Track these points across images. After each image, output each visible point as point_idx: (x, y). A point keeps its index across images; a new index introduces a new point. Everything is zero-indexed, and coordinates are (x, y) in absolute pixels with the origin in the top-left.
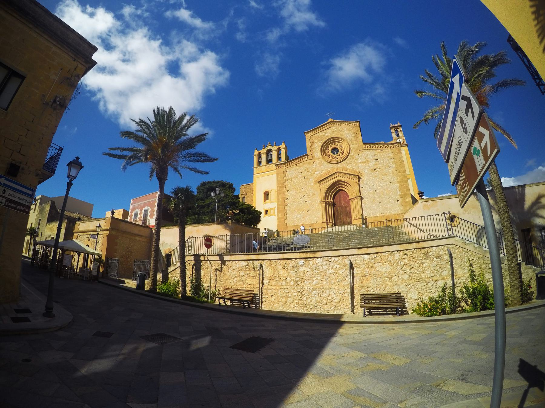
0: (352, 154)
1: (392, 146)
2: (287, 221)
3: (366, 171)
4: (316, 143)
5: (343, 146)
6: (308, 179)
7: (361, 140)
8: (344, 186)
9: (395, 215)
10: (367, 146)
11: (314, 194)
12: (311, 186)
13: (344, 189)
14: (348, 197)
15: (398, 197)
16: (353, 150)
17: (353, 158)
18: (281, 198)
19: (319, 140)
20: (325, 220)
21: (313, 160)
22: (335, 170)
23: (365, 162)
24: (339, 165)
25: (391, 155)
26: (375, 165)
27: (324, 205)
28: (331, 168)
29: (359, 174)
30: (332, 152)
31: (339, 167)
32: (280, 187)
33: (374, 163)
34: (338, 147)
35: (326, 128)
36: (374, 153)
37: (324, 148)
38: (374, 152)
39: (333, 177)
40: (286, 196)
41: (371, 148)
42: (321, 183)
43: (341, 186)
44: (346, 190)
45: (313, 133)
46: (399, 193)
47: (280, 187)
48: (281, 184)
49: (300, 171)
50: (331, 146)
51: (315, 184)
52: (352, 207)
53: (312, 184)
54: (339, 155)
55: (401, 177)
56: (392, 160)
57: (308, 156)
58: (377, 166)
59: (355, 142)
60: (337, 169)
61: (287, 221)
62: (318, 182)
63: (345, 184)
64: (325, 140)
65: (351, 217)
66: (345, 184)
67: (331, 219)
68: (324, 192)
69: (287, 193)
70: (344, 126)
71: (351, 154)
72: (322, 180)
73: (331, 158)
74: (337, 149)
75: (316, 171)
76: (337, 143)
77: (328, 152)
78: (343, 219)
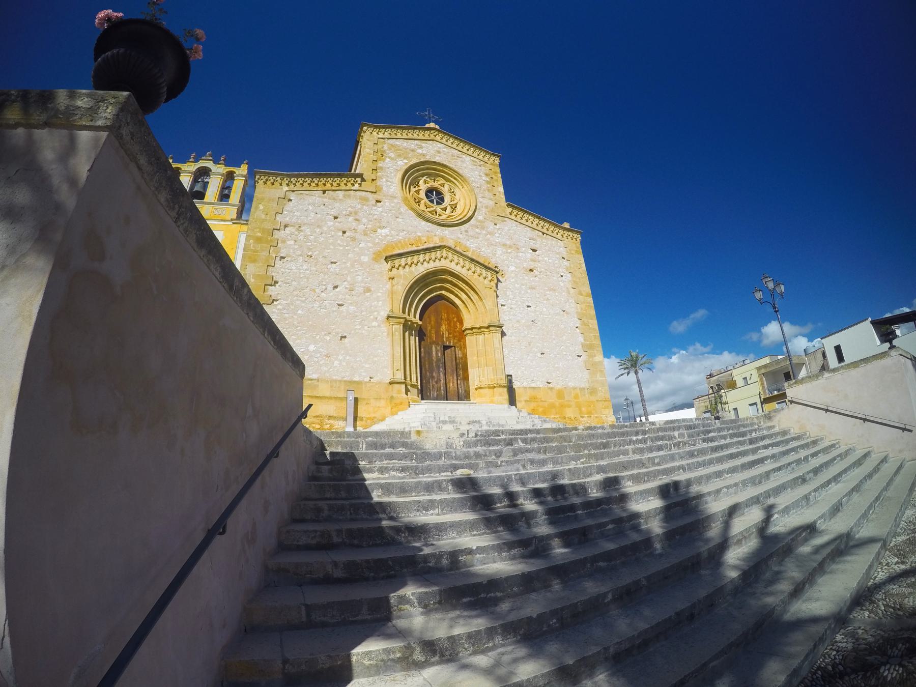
0: (480, 218)
1: (566, 233)
3: (512, 268)
4: (392, 159)
7: (503, 196)
8: (456, 290)
9: (575, 388)
10: (515, 212)
14: (461, 323)
15: (579, 350)
16: (484, 210)
17: (483, 228)
19: (400, 156)
20: (400, 376)
21: (376, 197)
24: (447, 231)
26: (534, 261)
30: (426, 195)
31: (449, 236)
32: (258, 240)
33: (529, 256)
34: (445, 190)
35: (421, 137)
37: (411, 175)
38: (529, 233)
39: (433, 255)
40: (274, 273)
41: (523, 221)
42: (397, 262)
43: (448, 286)
45: (387, 135)
47: (258, 240)
48: (263, 231)
49: (334, 212)
50: (425, 182)
52: (469, 351)
53: (365, 259)
54: (445, 209)
55: (583, 306)
57: (363, 180)
59: (487, 194)
60: (442, 239)
63: (460, 284)
64: (414, 161)
65: (466, 378)
66: (460, 284)
67: (415, 378)
68: (401, 288)
69: (279, 263)
70: (465, 150)
71: (479, 216)
72: (400, 255)
74: (439, 193)
76: (442, 181)
77: (418, 192)
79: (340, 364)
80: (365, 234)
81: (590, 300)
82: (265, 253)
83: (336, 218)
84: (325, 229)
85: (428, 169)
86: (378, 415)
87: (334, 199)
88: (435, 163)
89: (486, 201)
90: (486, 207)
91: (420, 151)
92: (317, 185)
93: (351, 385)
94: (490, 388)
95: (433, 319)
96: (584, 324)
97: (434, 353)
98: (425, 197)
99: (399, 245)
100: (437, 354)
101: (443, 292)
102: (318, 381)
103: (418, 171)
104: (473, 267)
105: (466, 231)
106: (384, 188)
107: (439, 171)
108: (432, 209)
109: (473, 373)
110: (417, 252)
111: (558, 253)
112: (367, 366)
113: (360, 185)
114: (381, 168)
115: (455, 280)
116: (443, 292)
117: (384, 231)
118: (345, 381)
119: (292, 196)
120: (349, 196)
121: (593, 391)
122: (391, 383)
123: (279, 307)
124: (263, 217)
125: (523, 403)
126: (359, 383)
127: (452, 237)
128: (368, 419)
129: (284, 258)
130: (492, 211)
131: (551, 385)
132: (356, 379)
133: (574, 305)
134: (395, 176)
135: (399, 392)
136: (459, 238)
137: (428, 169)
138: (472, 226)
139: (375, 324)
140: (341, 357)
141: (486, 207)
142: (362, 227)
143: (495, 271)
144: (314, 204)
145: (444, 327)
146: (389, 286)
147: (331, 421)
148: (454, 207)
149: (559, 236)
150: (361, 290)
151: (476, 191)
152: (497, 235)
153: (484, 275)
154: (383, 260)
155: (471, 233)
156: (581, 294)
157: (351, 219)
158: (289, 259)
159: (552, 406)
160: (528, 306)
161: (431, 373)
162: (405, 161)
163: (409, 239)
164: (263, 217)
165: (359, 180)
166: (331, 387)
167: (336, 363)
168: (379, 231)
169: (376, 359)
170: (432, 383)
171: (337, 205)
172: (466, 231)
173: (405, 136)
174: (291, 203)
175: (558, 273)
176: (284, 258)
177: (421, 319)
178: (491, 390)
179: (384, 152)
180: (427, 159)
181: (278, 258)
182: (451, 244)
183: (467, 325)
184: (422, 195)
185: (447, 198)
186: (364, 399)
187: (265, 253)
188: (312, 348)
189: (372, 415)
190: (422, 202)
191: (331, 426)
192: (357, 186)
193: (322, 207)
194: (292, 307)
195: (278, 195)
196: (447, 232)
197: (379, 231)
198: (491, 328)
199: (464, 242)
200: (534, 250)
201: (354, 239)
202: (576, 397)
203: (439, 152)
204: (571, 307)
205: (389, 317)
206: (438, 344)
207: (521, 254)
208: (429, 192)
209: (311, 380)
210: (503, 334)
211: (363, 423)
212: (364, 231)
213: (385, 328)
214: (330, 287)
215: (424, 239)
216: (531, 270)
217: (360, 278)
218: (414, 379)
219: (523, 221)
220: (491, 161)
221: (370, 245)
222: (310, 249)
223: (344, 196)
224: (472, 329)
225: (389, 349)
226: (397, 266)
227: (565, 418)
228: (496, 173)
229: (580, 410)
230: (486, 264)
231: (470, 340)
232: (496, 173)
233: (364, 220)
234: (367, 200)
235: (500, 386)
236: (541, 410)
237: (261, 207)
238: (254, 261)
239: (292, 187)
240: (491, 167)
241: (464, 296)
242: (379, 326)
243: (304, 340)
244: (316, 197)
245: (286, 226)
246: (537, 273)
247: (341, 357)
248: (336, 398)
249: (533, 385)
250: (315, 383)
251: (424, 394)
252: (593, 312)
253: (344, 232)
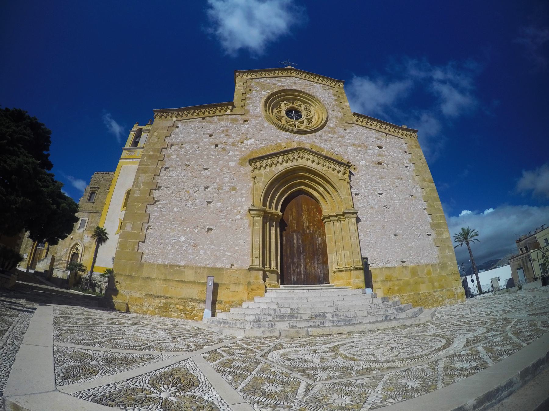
0: (332, 125)
1: (405, 133)
2: (144, 248)
3: (363, 163)
6: (224, 150)
8: (314, 184)
9: (427, 265)
11: (234, 189)
12: (229, 168)
13: (311, 191)
14: (320, 212)
15: (428, 229)
16: (334, 120)
17: (335, 133)
18: (145, 184)
19: (264, 88)
20: (258, 263)
21: (243, 117)
22: (295, 145)
24: (303, 138)
26: (380, 155)
27: (258, 220)
28: (284, 139)
30: (287, 114)
31: (306, 141)
33: (376, 152)
35: (280, 75)
36: (374, 136)
37: (272, 101)
40: (158, 180)
41: (368, 125)
42: (259, 164)
43: (306, 181)
45: (254, 76)
46: (429, 219)
47: (150, 157)
50: (285, 105)
51: (241, 164)
52: (329, 237)
55: (428, 190)
57: (234, 107)
59: (336, 108)
60: (300, 143)
61: (144, 248)
62: (252, 161)
65: (325, 262)
67: (275, 264)
69: (163, 172)
70: (315, 80)
72: (262, 158)
75: (247, 139)
76: (299, 103)
77: (280, 112)
78: (303, 265)
79: (205, 253)
80: (234, 145)
81: (433, 184)
82: (154, 166)
83: (211, 136)
84: (201, 144)
85: (286, 95)
86: (237, 299)
87: (211, 122)
88: (291, 90)
89: (335, 113)
90: (336, 117)
91: (280, 84)
92: (198, 114)
93: (214, 271)
94: (347, 270)
95: (294, 210)
96: (430, 206)
97: (295, 241)
98: (285, 115)
99: (262, 151)
100: (298, 241)
101: (303, 187)
102: (185, 267)
103: (278, 97)
104: (327, 164)
105: (320, 136)
106: (251, 111)
107: (296, 96)
108: (291, 123)
109: (331, 257)
110: (276, 155)
111: (401, 149)
112: (229, 254)
113: (231, 110)
114: (249, 98)
115: (312, 176)
116: (303, 187)
117: (249, 141)
118: (208, 268)
119: (179, 124)
120: (223, 119)
121: (443, 266)
122: (250, 270)
123: (160, 206)
124: (156, 140)
125: (380, 283)
126: (220, 269)
127: (309, 141)
128: (226, 302)
129: (167, 168)
130: (342, 119)
131: (405, 264)
132: (219, 266)
133: (419, 190)
134: (260, 102)
135: (257, 278)
136: (314, 142)
137: (286, 95)
138: (325, 132)
139: (238, 217)
140: (206, 247)
141: (336, 117)
142: (231, 140)
143: (348, 165)
144: (194, 128)
145: (304, 217)
146: (251, 185)
147: (193, 304)
148: (310, 120)
149: (400, 135)
150: (227, 189)
151: (327, 106)
152: (347, 137)
153: (338, 169)
154: (248, 164)
155: (324, 137)
156: (425, 180)
157: (222, 135)
158: (171, 169)
159: (407, 284)
160: (380, 194)
161: (292, 258)
162: (268, 91)
163: (271, 146)
164: (156, 140)
165: (230, 107)
166: (196, 273)
167: (202, 252)
168: (245, 142)
169: (237, 248)
170: (293, 267)
171: (213, 126)
172: (320, 136)
173: (267, 75)
174: (177, 129)
175: (403, 164)
176: (167, 168)
177: (281, 211)
178: (349, 272)
179: (252, 87)
180: (286, 88)
181: (163, 169)
182: (308, 147)
183: (325, 214)
184: (283, 114)
185: (304, 114)
186: (224, 284)
187: (154, 166)
188: (182, 239)
189: (231, 299)
190: (283, 119)
191: (193, 308)
192: (229, 111)
193: (201, 129)
194: (170, 206)
195: (168, 125)
196: (303, 138)
197: (245, 142)
198: (346, 215)
199: (319, 145)
200: (381, 148)
201: (224, 150)
202: (429, 273)
203: (295, 83)
204: (418, 192)
205: (250, 210)
206: (299, 232)
207: (369, 151)
208: (289, 112)
209: (179, 266)
210: (358, 220)
211: (222, 306)
212: (233, 143)
213: (247, 221)
214: (202, 188)
215: (284, 145)
216: (380, 163)
217: (227, 179)
218: (273, 265)
219: (368, 125)
220: (337, 86)
221: (237, 153)
222: (188, 160)
223: (219, 120)
224: (329, 217)
225: (250, 239)
226: (258, 167)
227: (419, 294)
228: (341, 93)
229: (433, 285)
230: (340, 160)
231: (329, 227)
232: (341, 93)
233: (234, 135)
234: (236, 120)
235: (357, 269)
236: (396, 288)
237: (156, 134)
238: (144, 172)
239: (179, 118)
240: (338, 90)
241: (321, 189)
242: (242, 218)
243: (176, 233)
244: (197, 123)
245: (172, 145)
246: (385, 165)
247: (206, 247)
248: (199, 283)
249: (389, 265)
250: (182, 269)
251: (284, 278)
252: (436, 195)
253: (217, 145)
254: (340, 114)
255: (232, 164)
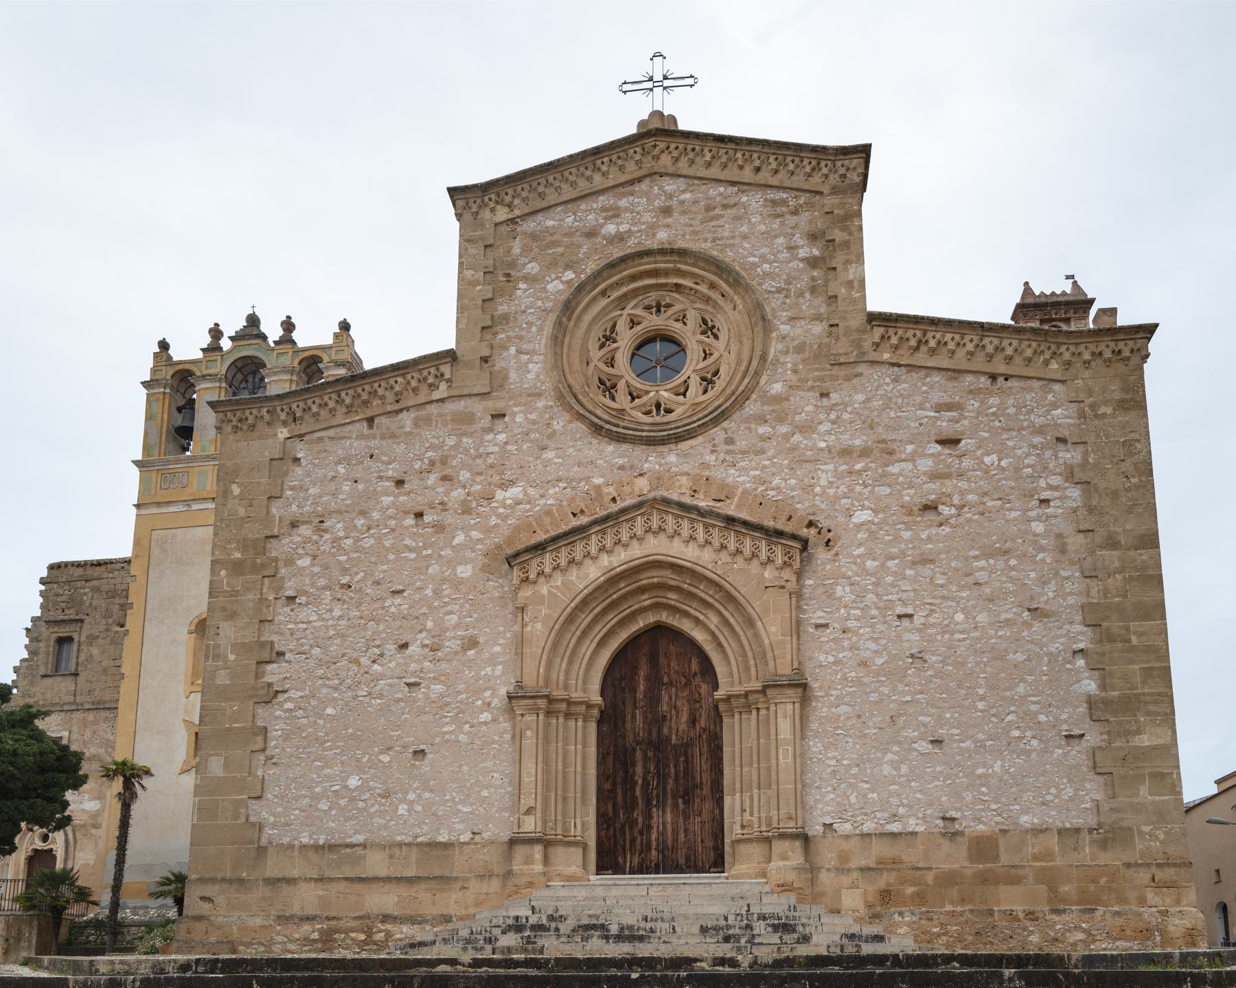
3: (862, 516)
5: (720, 322)
6: (439, 528)
12: (457, 584)
13: (686, 626)
17: (781, 419)
19: (552, 265)
23: (865, 452)
24: (671, 457)
25: (1063, 416)
26: (935, 476)
29: (804, 532)
33: (925, 465)
35: (615, 177)
36: (937, 397)
38: (937, 389)
44: (699, 636)
56: (1070, 456)
58: (948, 486)
64: (591, 267)
72: (540, 548)
73: (623, 400)
75: (504, 486)
80: (467, 511)
91: (611, 228)
155: (741, 444)
254: (818, 329)
255: (465, 571)
